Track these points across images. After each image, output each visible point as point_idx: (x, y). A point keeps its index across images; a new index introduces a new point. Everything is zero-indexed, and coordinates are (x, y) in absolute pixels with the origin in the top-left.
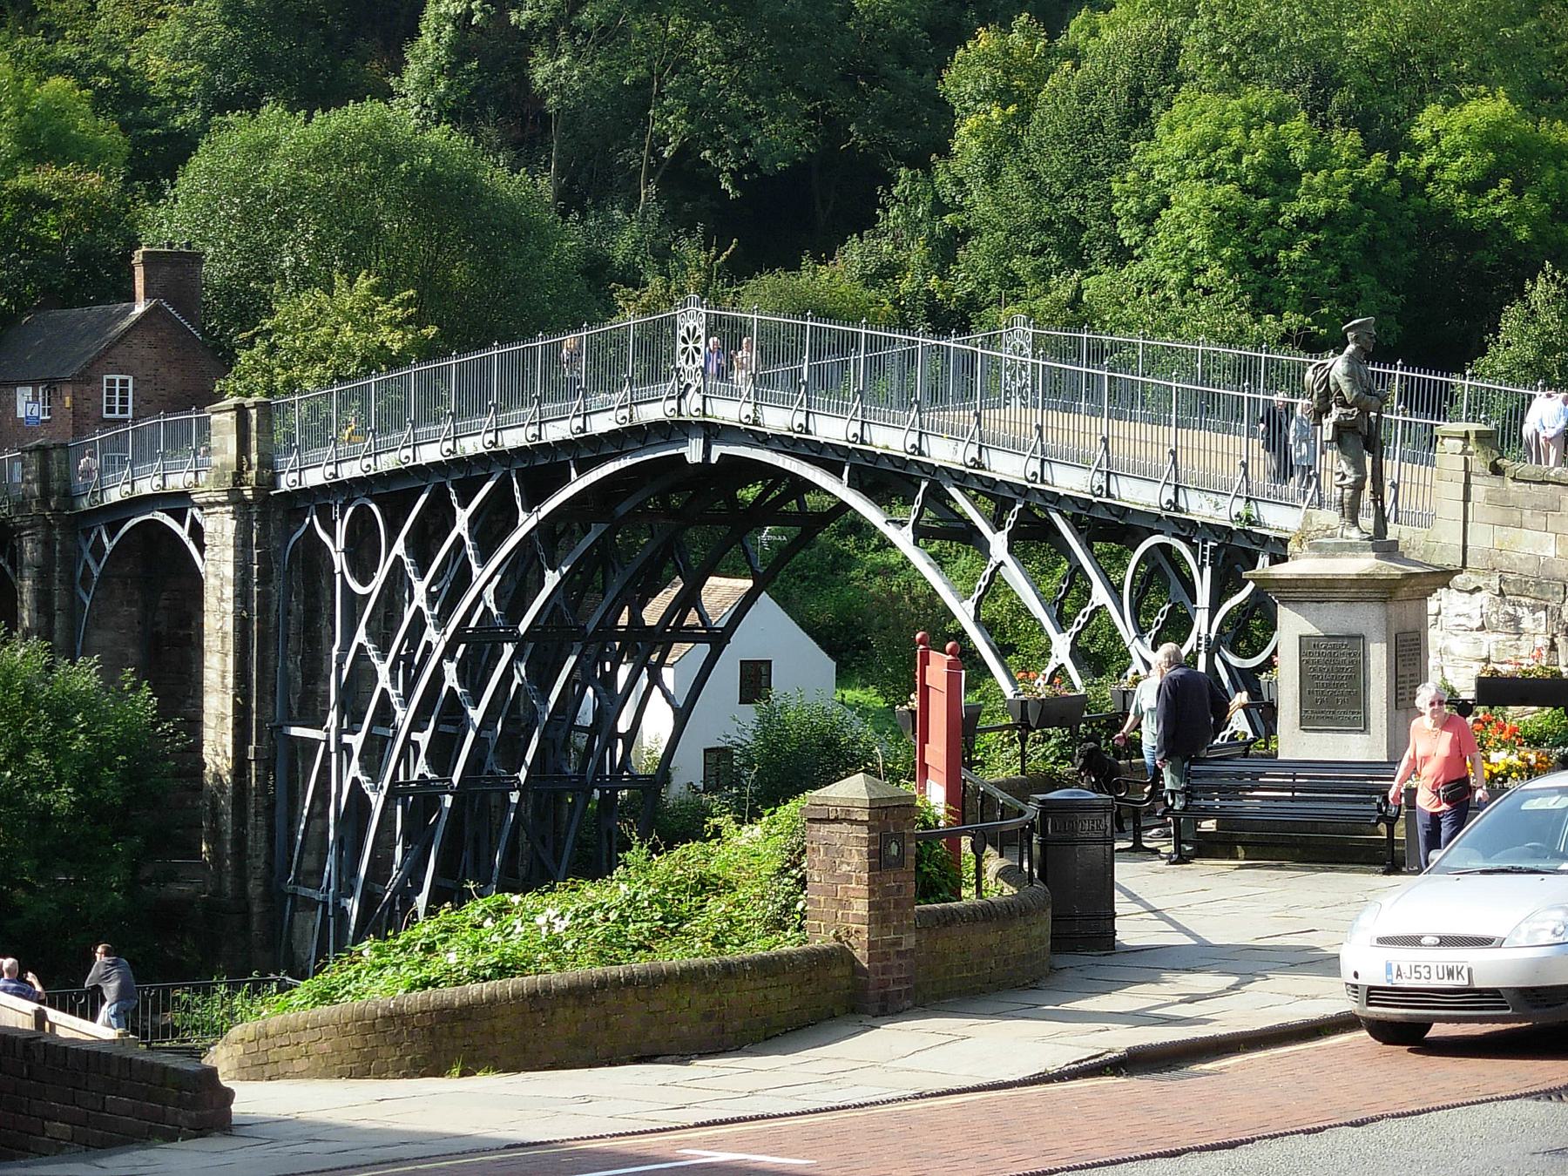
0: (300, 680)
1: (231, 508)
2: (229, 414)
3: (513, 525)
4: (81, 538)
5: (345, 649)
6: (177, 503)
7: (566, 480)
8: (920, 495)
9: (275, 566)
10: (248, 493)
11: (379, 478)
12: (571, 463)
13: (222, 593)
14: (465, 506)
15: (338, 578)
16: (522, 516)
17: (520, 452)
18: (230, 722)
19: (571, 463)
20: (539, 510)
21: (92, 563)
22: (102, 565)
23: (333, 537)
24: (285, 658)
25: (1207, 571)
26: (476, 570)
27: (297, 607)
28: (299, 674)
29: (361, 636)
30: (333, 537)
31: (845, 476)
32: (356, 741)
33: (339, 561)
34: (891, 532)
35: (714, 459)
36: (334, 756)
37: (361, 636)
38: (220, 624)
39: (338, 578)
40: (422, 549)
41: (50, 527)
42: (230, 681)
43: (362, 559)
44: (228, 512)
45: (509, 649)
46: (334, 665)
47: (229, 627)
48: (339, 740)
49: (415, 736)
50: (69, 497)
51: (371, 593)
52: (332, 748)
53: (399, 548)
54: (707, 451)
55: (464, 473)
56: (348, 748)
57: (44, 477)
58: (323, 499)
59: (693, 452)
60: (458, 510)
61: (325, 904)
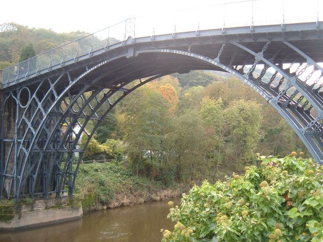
3: (68, 84)
5: (19, 120)
7: (85, 71)
11: (30, 80)
14: (53, 83)
17: (71, 65)
23: (16, 98)
26: (56, 97)
29: (24, 117)
30: (16, 98)
32: (22, 141)
33: (18, 102)
34: (210, 61)
35: (137, 55)
37: (24, 117)
39: (18, 106)
40: (40, 96)
43: (24, 102)
53: (34, 96)
54: (134, 53)
55: (53, 74)
56: (19, 143)
58: (13, 89)
59: (130, 54)
61: (13, 177)
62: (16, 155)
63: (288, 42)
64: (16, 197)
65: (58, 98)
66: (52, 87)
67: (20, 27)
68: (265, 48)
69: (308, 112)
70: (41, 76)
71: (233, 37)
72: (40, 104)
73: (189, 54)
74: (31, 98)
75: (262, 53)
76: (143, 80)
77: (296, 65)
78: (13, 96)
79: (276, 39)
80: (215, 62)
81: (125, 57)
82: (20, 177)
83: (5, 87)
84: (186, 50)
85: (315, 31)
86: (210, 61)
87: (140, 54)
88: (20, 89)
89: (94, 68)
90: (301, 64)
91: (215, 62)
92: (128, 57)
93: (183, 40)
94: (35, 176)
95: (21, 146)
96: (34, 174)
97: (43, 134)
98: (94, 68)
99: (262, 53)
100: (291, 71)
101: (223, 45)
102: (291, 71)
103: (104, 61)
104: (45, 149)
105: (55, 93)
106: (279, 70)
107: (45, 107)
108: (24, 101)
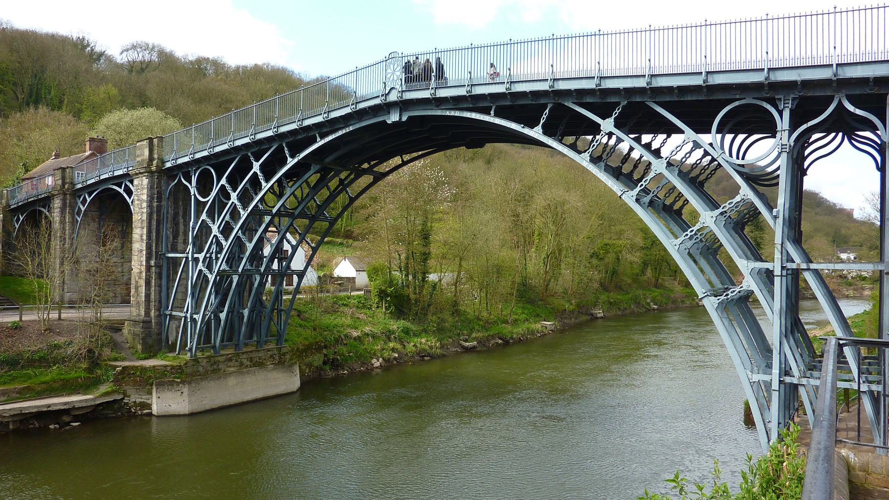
0: (171, 238)
1: (146, 174)
2: (146, 141)
3: (284, 162)
4: (78, 199)
5: (196, 223)
6: (118, 180)
7: (315, 141)
8: (547, 111)
9: (163, 196)
10: (154, 168)
12: (317, 135)
13: (141, 206)
15: (193, 197)
16: (289, 159)
18: (144, 252)
19: (317, 135)
20: (299, 156)
21: (81, 206)
22: (85, 207)
23: (191, 185)
24: (167, 229)
25: (786, 114)
26: (264, 184)
27: (171, 211)
28: (171, 236)
29: (204, 216)
30: (191, 185)
31: (492, 112)
32: (201, 256)
33: (193, 190)
34: (527, 131)
35: (404, 119)
36: (191, 263)
38: (140, 217)
39: (193, 197)
40: (234, 181)
41: (65, 194)
42: (145, 237)
43: (204, 189)
44: (144, 176)
45: (267, 219)
46: (191, 229)
47: (145, 217)
48: (192, 256)
49: (219, 255)
50: (73, 184)
52: (190, 259)
53: (223, 181)
54: (400, 116)
55: (258, 148)
56: (196, 260)
57: (63, 178)
58: (185, 170)
59: (394, 117)
60: (254, 163)
61: (186, 317)
62: (193, 276)
63: (654, 102)
64: (191, 350)
65: (266, 186)
66: (256, 167)
67: (162, 53)
69: (679, 213)
70: (237, 149)
71: (567, 93)
72: (234, 196)
76: (406, 157)
77: (662, 137)
78: (183, 179)
79: (638, 99)
80: (536, 133)
81: (385, 121)
82: (198, 317)
83: (168, 165)
84: (489, 114)
85: (700, 86)
86: (527, 131)
87: (410, 118)
88: (195, 171)
89: (330, 138)
90: (669, 136)
91: (536, 133)
92: (389, 122)
93: (482, 97)
94: (223, 316)
95: (200, 265)
96: (222, 312)
97: (239, 245)
98: (330, 138)
100: (655, 146)
102: (655, 146)
103: (348, 126)
104: (240, 270)
105: (261, 177)
106: (635, 145)
107: (245, 198)
108: (205, 187)
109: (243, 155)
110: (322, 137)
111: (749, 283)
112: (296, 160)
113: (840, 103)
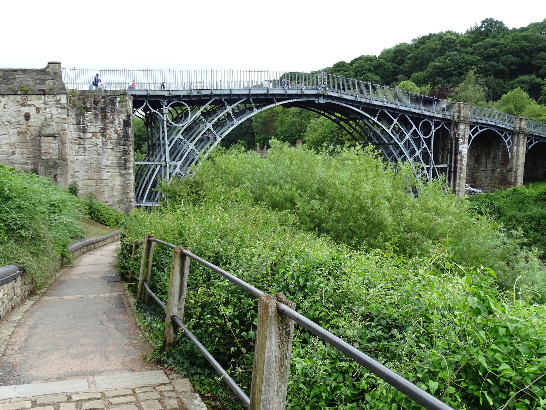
7: (273, 103)
12: (275, 99)
19: (275, 99)
31: (361, 109)
34: (372, 118)
35: (324, 103)
51: (183, 126)
59: (322, 101)
60: (227, 106)
68: (398, 117)
73: (361, 112)
74: (191, 117)
75: (397, 119)
80: (375, 120)
84: (358, 108)
86: (372, 118)
92: (317, 102)
99: (397, 119)
101: (380, 111)
109: (215, 99)
110: (278, 101)
111: (425, 172)
112: (259, 111)
113: (443, 125)
